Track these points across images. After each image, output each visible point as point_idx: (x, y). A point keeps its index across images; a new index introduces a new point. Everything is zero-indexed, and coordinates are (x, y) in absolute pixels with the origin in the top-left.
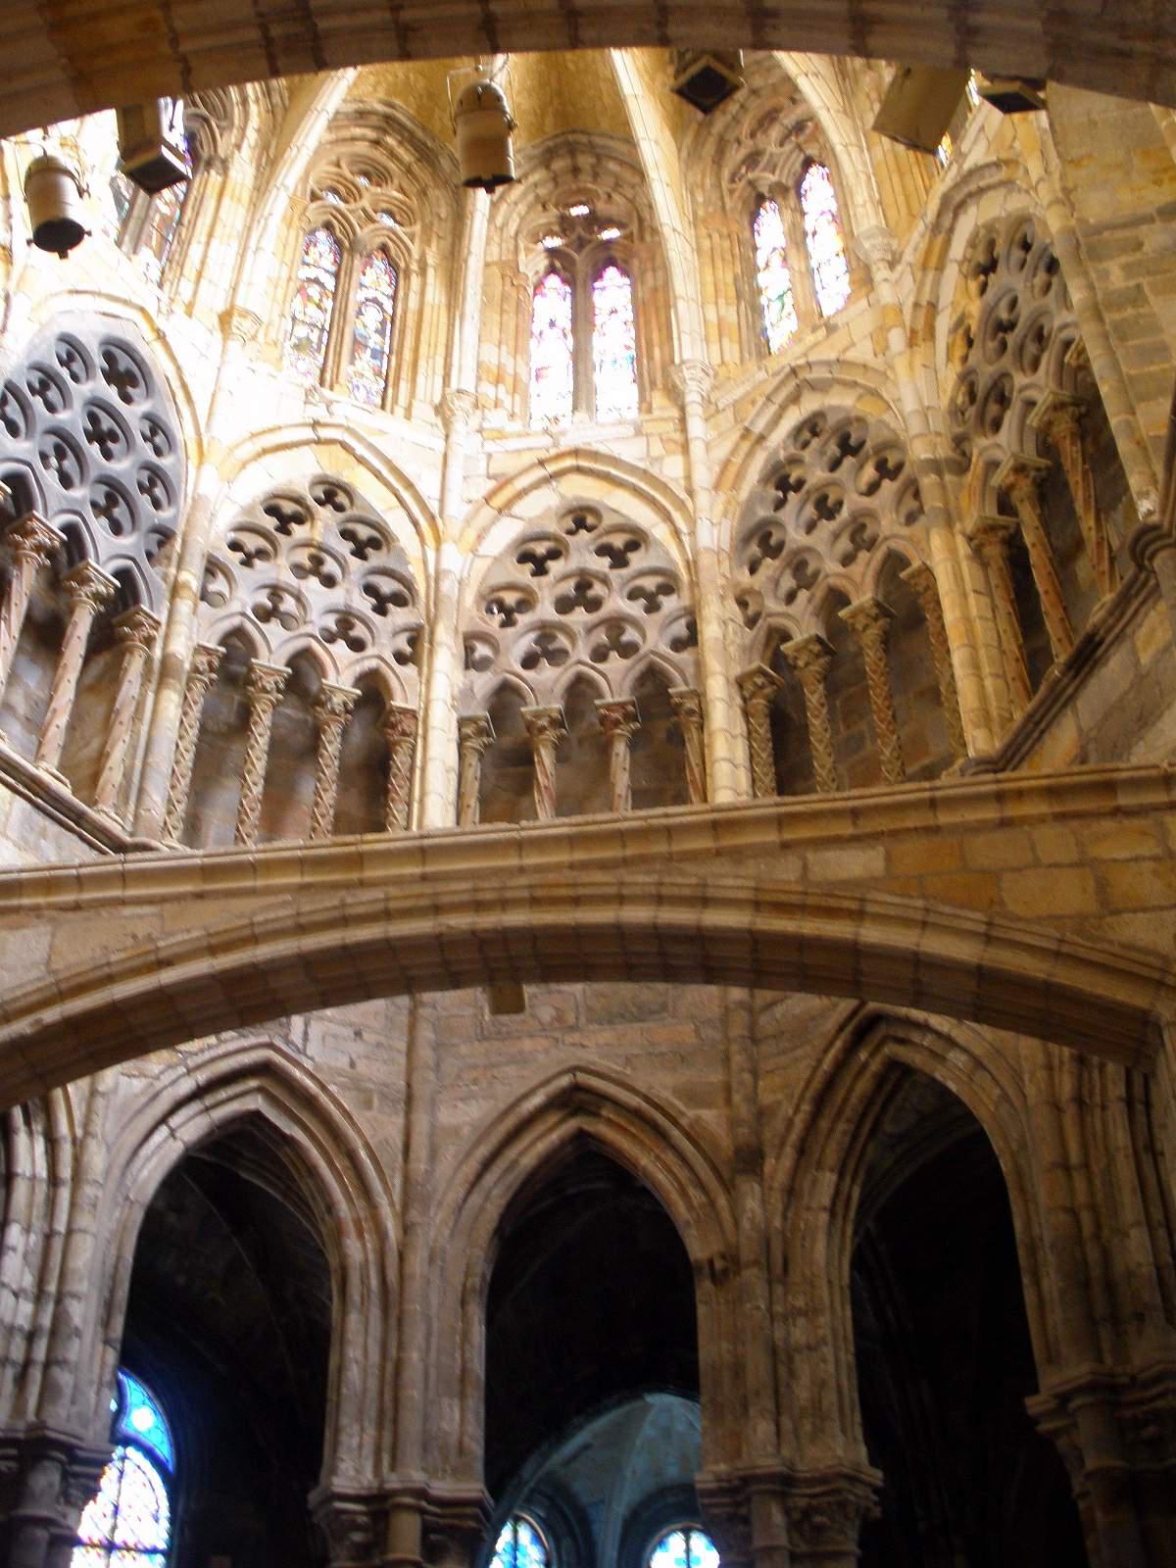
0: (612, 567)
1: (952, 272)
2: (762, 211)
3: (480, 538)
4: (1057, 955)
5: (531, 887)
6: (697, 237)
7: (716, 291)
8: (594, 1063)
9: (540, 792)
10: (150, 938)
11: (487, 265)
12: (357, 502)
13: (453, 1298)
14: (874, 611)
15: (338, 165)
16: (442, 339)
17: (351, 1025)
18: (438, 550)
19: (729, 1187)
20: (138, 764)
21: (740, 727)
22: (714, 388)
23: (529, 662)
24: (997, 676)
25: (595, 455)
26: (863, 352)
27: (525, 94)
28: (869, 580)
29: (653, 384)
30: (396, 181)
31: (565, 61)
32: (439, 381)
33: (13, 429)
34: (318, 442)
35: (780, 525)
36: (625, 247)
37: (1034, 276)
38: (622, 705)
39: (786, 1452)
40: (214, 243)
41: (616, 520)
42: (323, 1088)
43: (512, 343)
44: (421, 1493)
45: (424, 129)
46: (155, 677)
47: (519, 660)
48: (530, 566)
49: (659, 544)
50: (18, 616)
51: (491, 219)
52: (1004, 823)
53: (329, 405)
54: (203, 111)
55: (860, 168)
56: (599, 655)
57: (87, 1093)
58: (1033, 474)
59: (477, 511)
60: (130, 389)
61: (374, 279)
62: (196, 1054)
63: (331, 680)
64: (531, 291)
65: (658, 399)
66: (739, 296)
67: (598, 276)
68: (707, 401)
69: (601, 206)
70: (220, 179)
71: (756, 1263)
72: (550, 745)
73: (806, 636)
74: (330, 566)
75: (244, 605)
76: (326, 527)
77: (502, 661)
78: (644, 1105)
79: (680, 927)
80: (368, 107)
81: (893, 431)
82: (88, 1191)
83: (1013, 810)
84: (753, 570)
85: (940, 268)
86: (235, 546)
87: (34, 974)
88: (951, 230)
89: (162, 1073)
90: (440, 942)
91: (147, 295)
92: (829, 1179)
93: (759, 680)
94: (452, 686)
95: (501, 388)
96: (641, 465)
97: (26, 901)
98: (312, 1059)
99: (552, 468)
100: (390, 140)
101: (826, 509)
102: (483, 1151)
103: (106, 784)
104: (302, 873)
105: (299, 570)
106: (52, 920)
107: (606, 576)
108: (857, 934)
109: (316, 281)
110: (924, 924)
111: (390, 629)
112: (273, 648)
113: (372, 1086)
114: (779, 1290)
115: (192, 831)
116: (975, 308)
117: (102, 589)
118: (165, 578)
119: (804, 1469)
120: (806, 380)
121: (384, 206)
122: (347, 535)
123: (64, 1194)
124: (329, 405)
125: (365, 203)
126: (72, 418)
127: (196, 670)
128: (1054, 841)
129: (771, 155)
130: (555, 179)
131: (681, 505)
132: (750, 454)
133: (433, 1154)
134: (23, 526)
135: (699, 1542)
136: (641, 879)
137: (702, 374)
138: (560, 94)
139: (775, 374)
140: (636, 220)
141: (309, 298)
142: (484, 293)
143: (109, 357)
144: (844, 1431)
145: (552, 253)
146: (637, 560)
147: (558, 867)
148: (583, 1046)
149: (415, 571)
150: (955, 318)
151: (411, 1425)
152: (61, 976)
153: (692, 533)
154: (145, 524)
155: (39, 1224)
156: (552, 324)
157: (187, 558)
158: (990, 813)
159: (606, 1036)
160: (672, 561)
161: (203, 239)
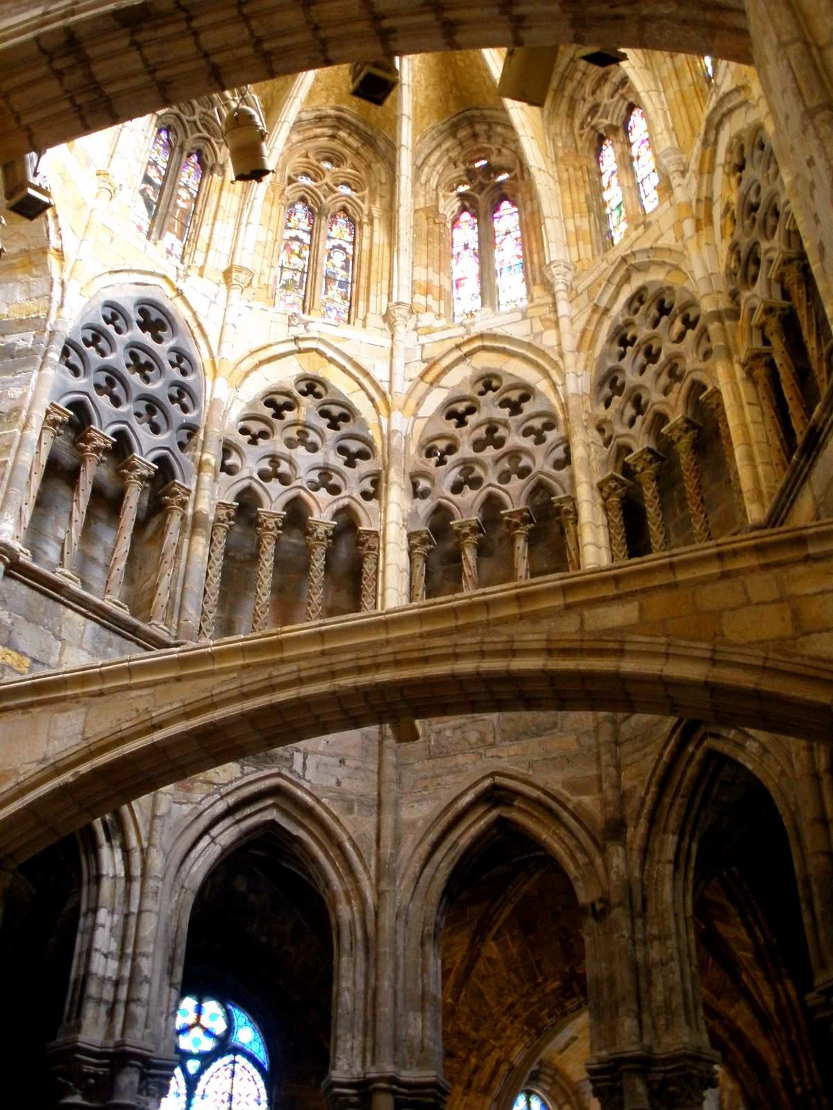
0: (511, 414)
1: (719, 173)
2: (604, 147)
3: (418, 405)
4: (764, 669)
5: (394, 653)
6: (558, 172)
7: (573, 208)
8: (506, 769)
9: (466, 580)
10: (147, 711)
11: (416, 211)
12: (330, 390)
13: (415, 942)
14: (685, 426)
15: (307, 157)
16: (386, 267)
17: (337, 755)
18: (389, 417)
19: (602, 850)
20: (179, 589)
21: (601, 519)
22: (575, 278)
23: (457, 488)
24: (767, 463)
25: (494, 337)
26: (668, 240)
27: (431, 88)
28: (680, 403)
29: (534, 280)
30: (349, 161)
31: (455, 60)
32: (385, 297)
33: (75, 371)
34: (300, 351)
35: (620, 370)
36: (511, 185)
37: (768, 168)
38: (520, 512)
39: (646, 1041)
40: (217, 223)
41: (512, 381)
42: (318, 801)
43: (436, 265)
44: (393, 1080)
45: (365, 122)
46: (189, 529)
47: (449, 488)
48: (454, 421)
49: (542, 394)
50: (85, 497)
51: (416, 178)
52: (725, 576)
53: (306, 324)
54: (205, 134)
55: (658, 106)
56: (505, 477)
57: (149, 815)
58: (778, 313)
59: (416, 386)
60: (160, 332)
61: (340, 232)
62: (226, 785)
63: (316, 516)
64: (449, 225)
65: (537, 291)
66: (590, 210)
68: (570, 288)
69: (495, 159)
70: (220, 178)
71: (621, 904)
72: (472, 546)
73: (641, 449)
74: (313, 437)
75: (251, 472)
76: (308, 410)
77: (437, 490)
78: (543, 797)
79: (496, 672)
80: (324, 113)
81: (691, 293)
82: (151, 883)
83: (731, 565)
84: (607, 405)
85: (711, 172)
86: (244, 431)
87: (74, 742)
88: (716, 142)
89: (203, 799)
90: (336, 697)
91: (169, 266)
92: (672, 840)
93: (613, 484)
94: (402, 511)
95: (430, 297)
96: (526, 340)
97: (69, 693)
98: (309, 781)
99: (466, 349)
100: (342, 134)
101: (652, 356)
102: (432, 837)
103: (157, 604)
104: (244, 657)
105: (290, 444)
106: (86, 704)
107: (506, 421)
108: (618, 667)
109: (296, 239)
110: (667, 655)
111: (357, 476)
112: (273, 498)
113: (353, 797)
114: (639, 922)
115: (227, 627)
116: (734, 198)
117: (145, 472)
118: (193, 459)
119: (660, 1051)
120: (632, 265)
121: (342, 180)
122: (324, 414)
123: (136, 886)
124: (306, 324)
125: (328, 179)
126: (118, 358)
127: (218, 520)
128: (762, 586)
129: (606, 105)
130: (461, 144)
131: (555, 365)
132: (600, 322)
133: (397, 841)
134: (85, 436)
136: (468, 641)
137: (566, 270)
138: (456, 84)
139: (612, 264)
140: (518, 165)
141: (292, 251)
142: (415, 232)
143: (142, 312)
144: (688, 1022)
145: (462, 196)
146: (528, 408)
147: (412, 637)
148: (500, 757)
149: (373, 432)
150: (723, 206)
151: (385, 1031)
152: (92, 741)
153: (564, 384)
154: (176, 424)
155: (120, 908)
156: (466, 247)
157: (208, 444)
158: (714, 569)
159: (515, 748)
160: (552, 405)
161: (210, 221)
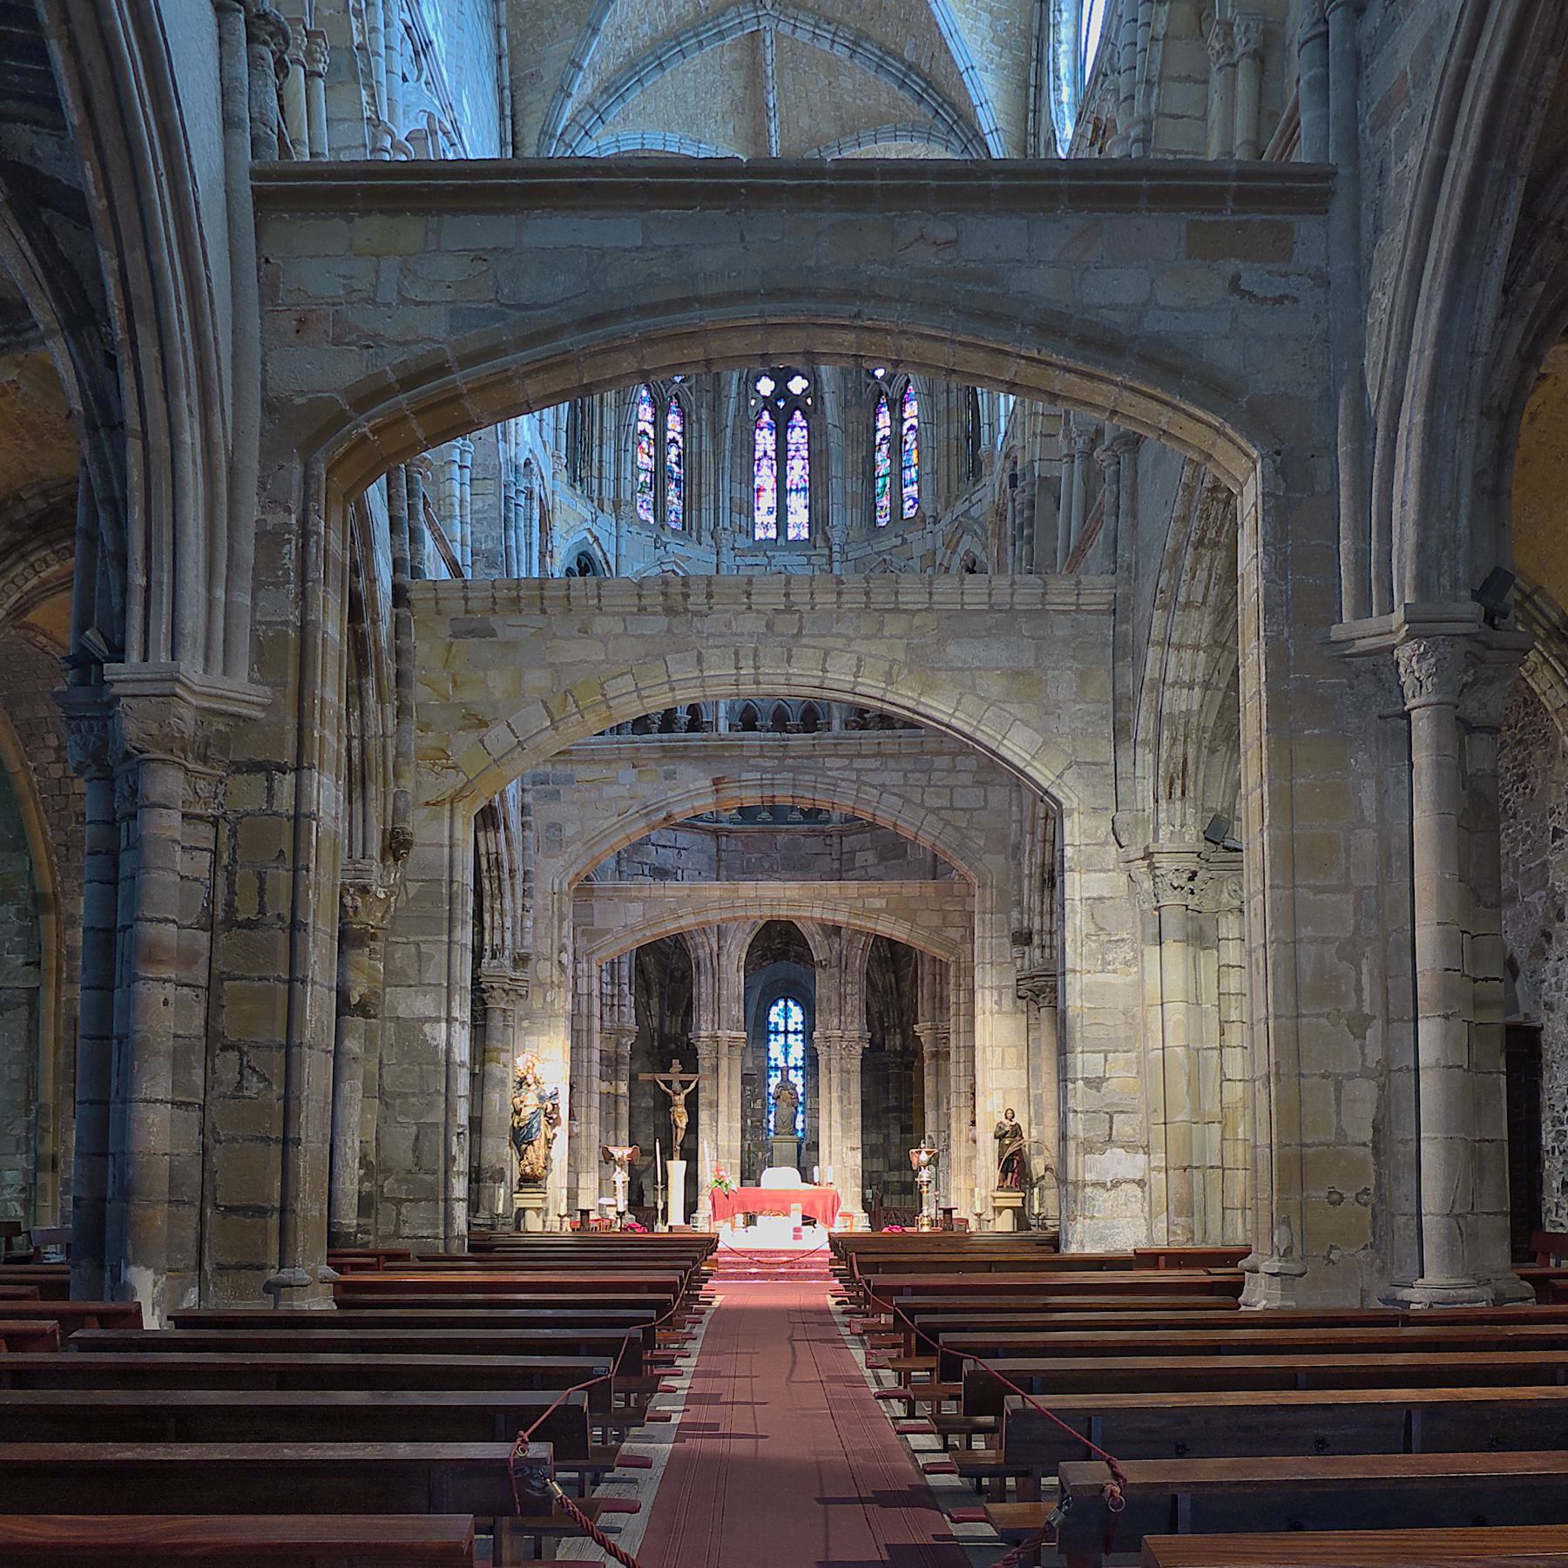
66: (864, 473)
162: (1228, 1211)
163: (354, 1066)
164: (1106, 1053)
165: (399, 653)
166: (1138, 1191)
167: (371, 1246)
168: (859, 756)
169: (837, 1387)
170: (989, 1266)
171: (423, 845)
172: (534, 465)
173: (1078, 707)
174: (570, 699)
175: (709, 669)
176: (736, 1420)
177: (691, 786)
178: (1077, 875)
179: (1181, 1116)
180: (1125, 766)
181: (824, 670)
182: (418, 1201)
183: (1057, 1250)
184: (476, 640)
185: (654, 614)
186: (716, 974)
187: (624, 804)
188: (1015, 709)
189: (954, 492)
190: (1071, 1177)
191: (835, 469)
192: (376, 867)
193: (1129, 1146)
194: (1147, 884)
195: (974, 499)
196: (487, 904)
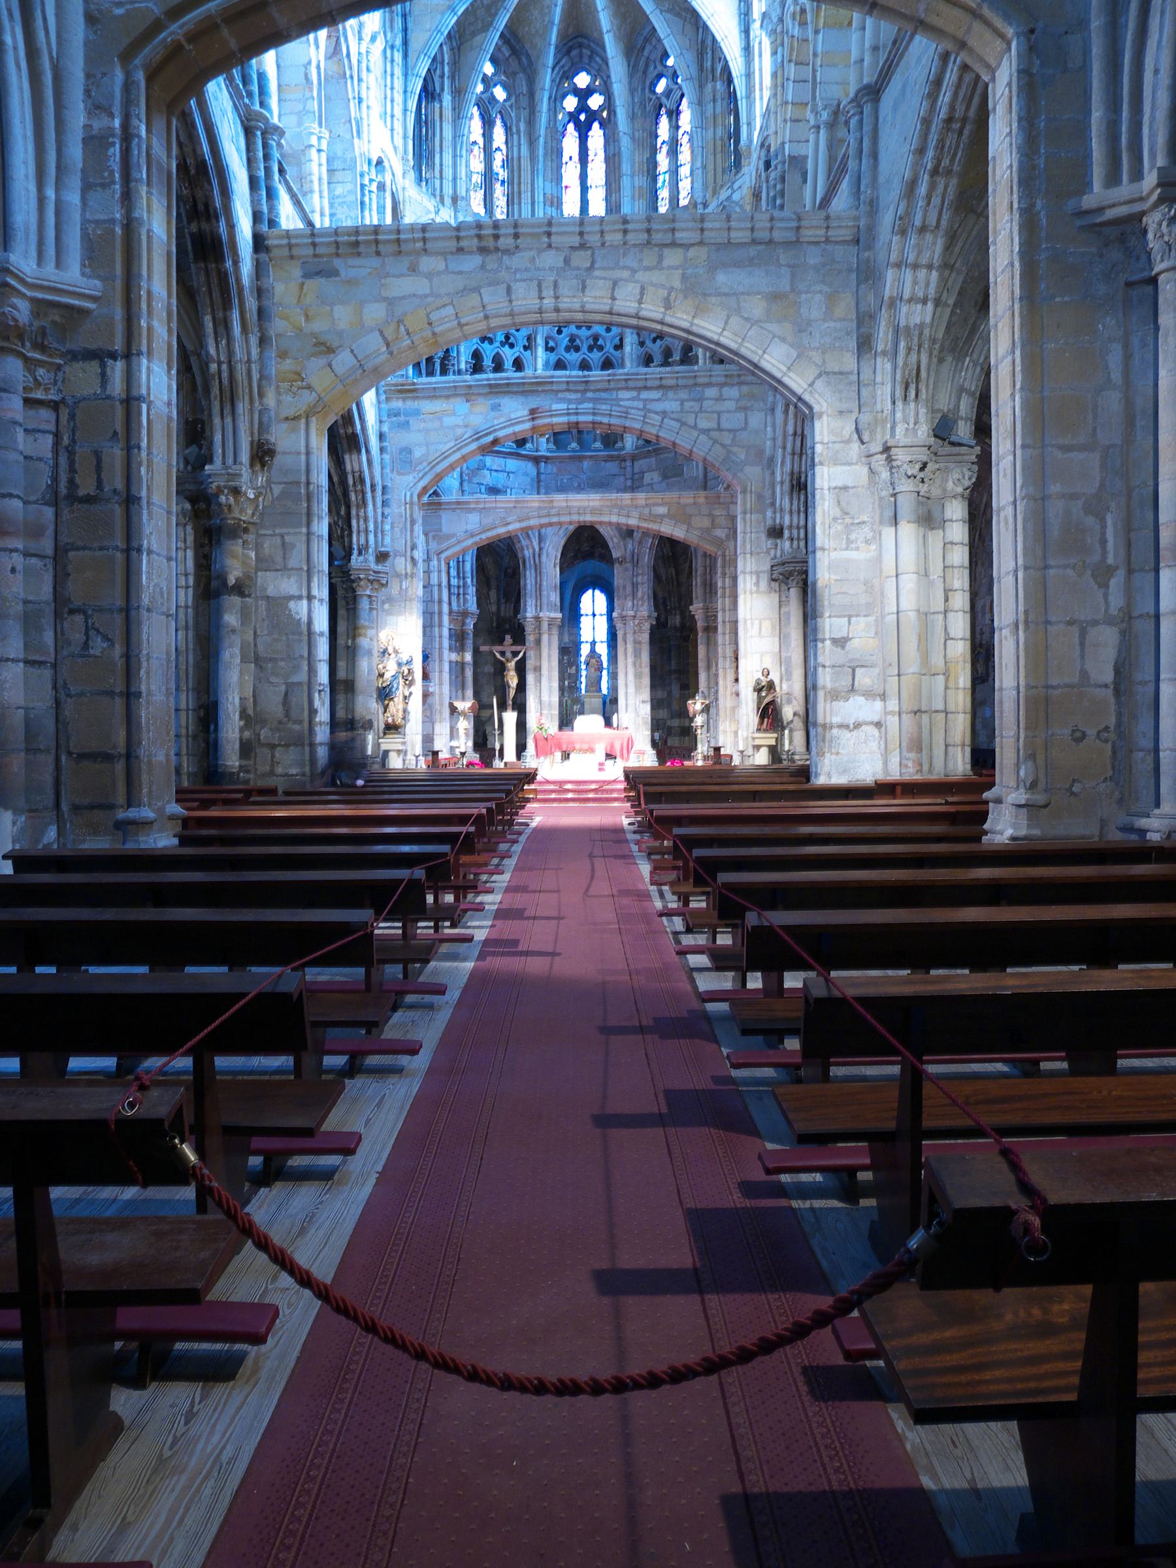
67: (590, 129)
109: (475, 143)
130: (572, 59)
135: (597, 592)
151: (545, 600)
162: (950, 748)
163: (233, 637)
164: (850, 617)
165: (260, 292)
166: (876, 732)
167: (252, 783)
168: (646, 388)
169: (625, 901)
170: (755, 796)
171: (284, 453)
172: (386, 164)
173: (827, 325)
174: (402, 328)
175: (517, 299)
176: (536, 935)
177: (513, 416)
178: (825, 469)
179: (912, 666)
180: (866, 376)
181: (613, 298)
182: (287, 746)
183: (808, 780)
184: (323, 280)
185: (470, 253)
186: (538, 569)
187: (459, 431)
188: (774, 327)
189: (719, 182)
190: (820, 720)
191: (626, 167)
192: (245, 472)
193: (869, 694)
194: (885, 475)
195: (736, 186)
196: (354, 512)
